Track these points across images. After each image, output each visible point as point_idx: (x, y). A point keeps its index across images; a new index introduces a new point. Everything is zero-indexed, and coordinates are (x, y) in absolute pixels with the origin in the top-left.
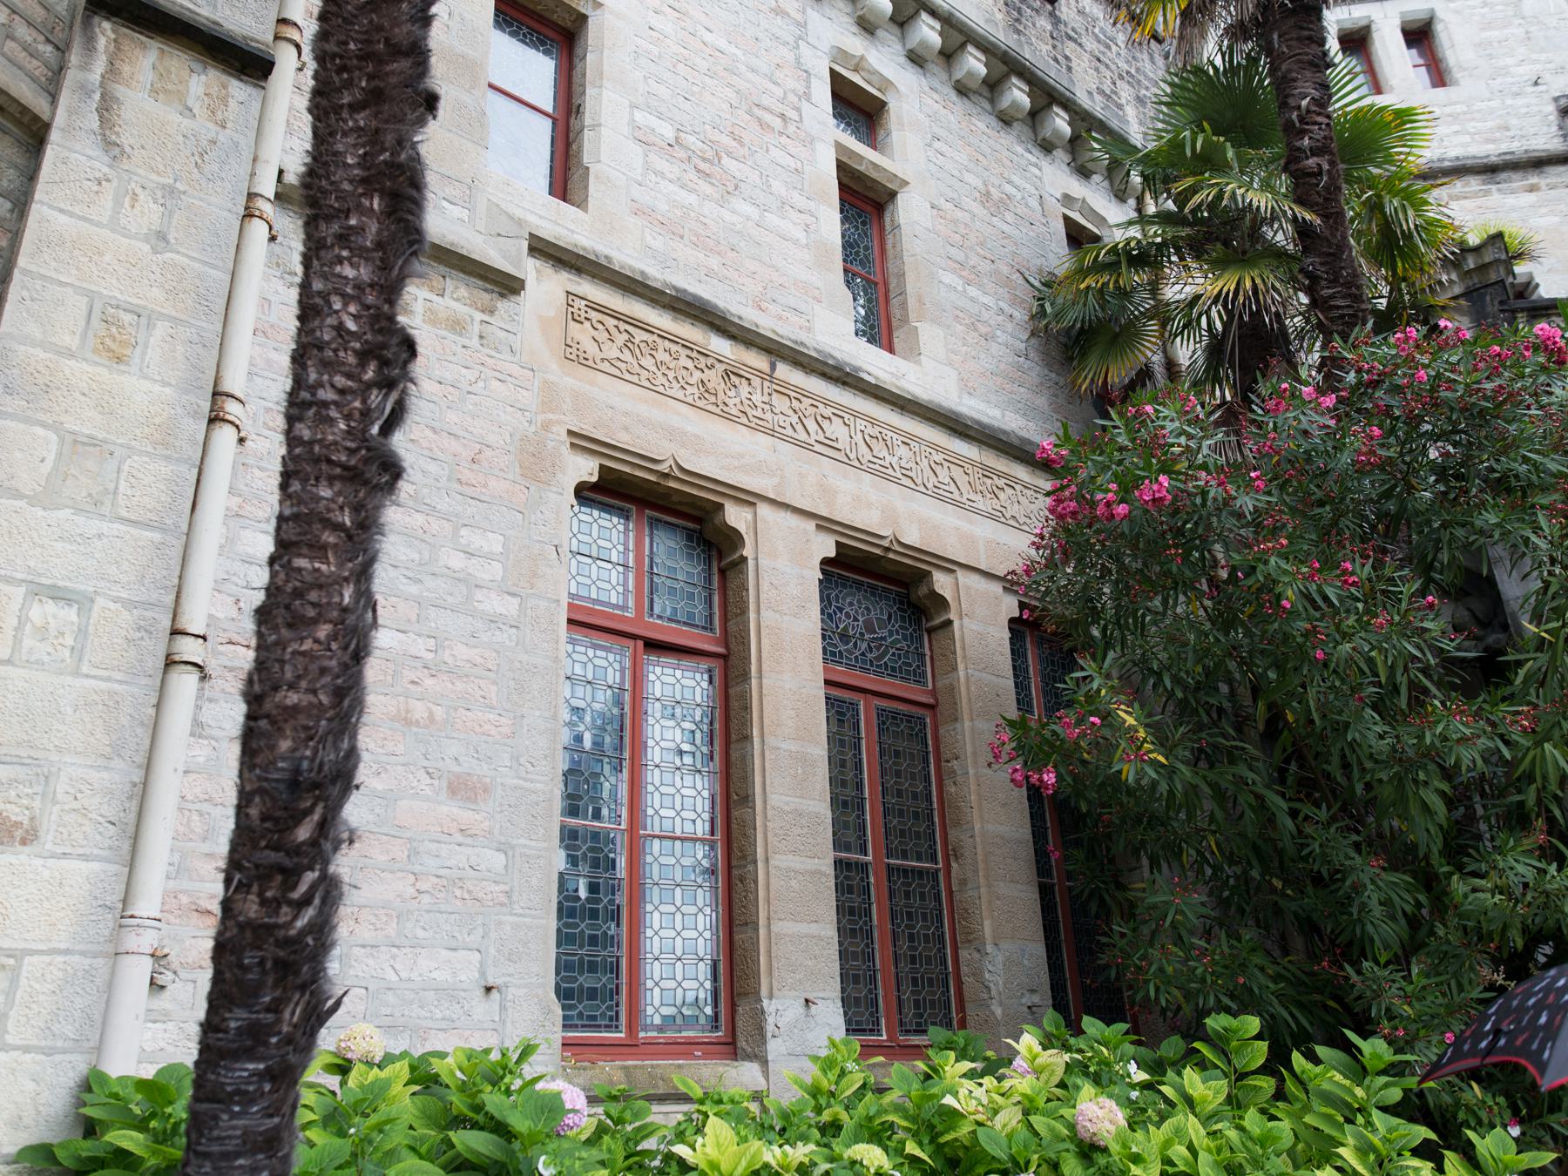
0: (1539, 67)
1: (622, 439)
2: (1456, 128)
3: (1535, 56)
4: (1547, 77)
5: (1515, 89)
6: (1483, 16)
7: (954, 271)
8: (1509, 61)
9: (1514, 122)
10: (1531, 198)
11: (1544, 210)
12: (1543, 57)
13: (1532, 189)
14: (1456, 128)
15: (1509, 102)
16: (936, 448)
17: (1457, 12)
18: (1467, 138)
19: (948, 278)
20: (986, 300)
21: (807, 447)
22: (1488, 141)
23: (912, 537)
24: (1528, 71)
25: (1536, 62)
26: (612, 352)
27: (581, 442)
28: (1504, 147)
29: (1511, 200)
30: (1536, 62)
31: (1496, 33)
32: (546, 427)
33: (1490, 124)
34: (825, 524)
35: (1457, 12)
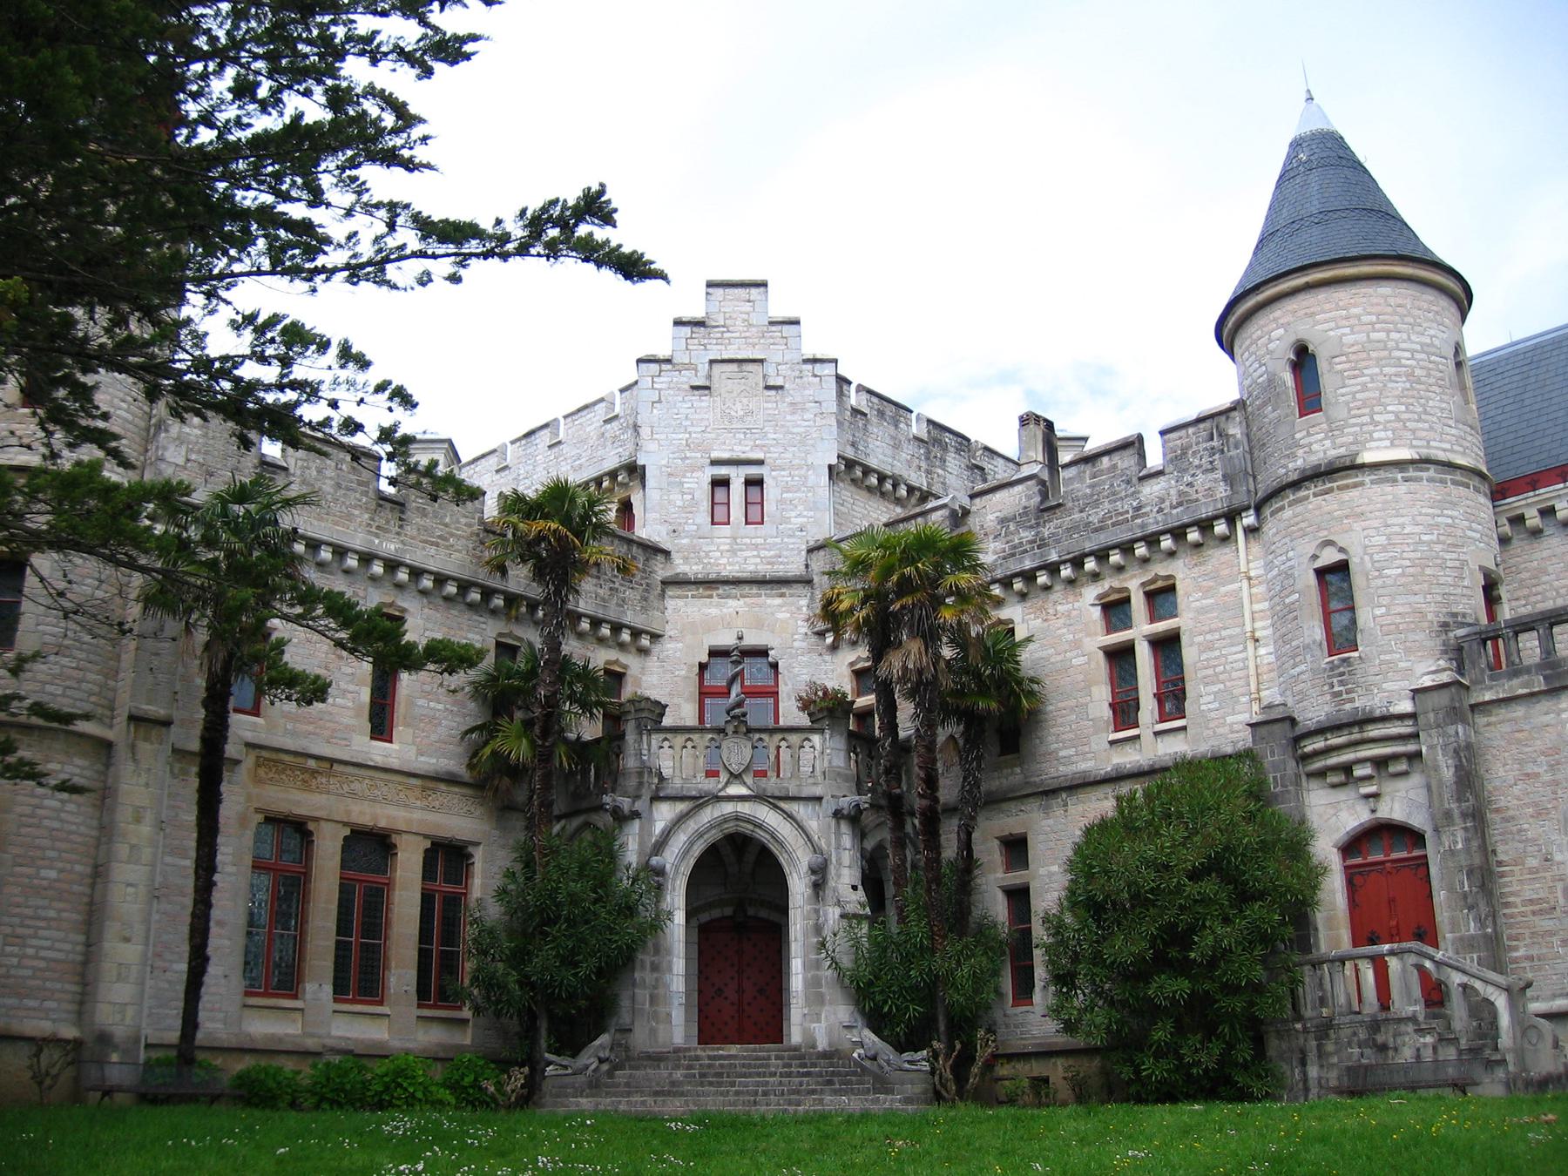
1: (273, 807)
7: (424, 697)
8: (793, 514)
10: (778, 601)
13: (782, 595)
16: (400, 783)
17: (774, 478)
18: (758, 560)
19: (421, 702)
20: (440, 707)
21: (342, 795)
22: (769, 563)
23: (382, 824)
26: (271, 775)
27: (258, 810)
29: (769, 601)
31: (789, 495)
32: (247, 808)
33: (772, 553)
34: (345, 824)
35: (774, 478)
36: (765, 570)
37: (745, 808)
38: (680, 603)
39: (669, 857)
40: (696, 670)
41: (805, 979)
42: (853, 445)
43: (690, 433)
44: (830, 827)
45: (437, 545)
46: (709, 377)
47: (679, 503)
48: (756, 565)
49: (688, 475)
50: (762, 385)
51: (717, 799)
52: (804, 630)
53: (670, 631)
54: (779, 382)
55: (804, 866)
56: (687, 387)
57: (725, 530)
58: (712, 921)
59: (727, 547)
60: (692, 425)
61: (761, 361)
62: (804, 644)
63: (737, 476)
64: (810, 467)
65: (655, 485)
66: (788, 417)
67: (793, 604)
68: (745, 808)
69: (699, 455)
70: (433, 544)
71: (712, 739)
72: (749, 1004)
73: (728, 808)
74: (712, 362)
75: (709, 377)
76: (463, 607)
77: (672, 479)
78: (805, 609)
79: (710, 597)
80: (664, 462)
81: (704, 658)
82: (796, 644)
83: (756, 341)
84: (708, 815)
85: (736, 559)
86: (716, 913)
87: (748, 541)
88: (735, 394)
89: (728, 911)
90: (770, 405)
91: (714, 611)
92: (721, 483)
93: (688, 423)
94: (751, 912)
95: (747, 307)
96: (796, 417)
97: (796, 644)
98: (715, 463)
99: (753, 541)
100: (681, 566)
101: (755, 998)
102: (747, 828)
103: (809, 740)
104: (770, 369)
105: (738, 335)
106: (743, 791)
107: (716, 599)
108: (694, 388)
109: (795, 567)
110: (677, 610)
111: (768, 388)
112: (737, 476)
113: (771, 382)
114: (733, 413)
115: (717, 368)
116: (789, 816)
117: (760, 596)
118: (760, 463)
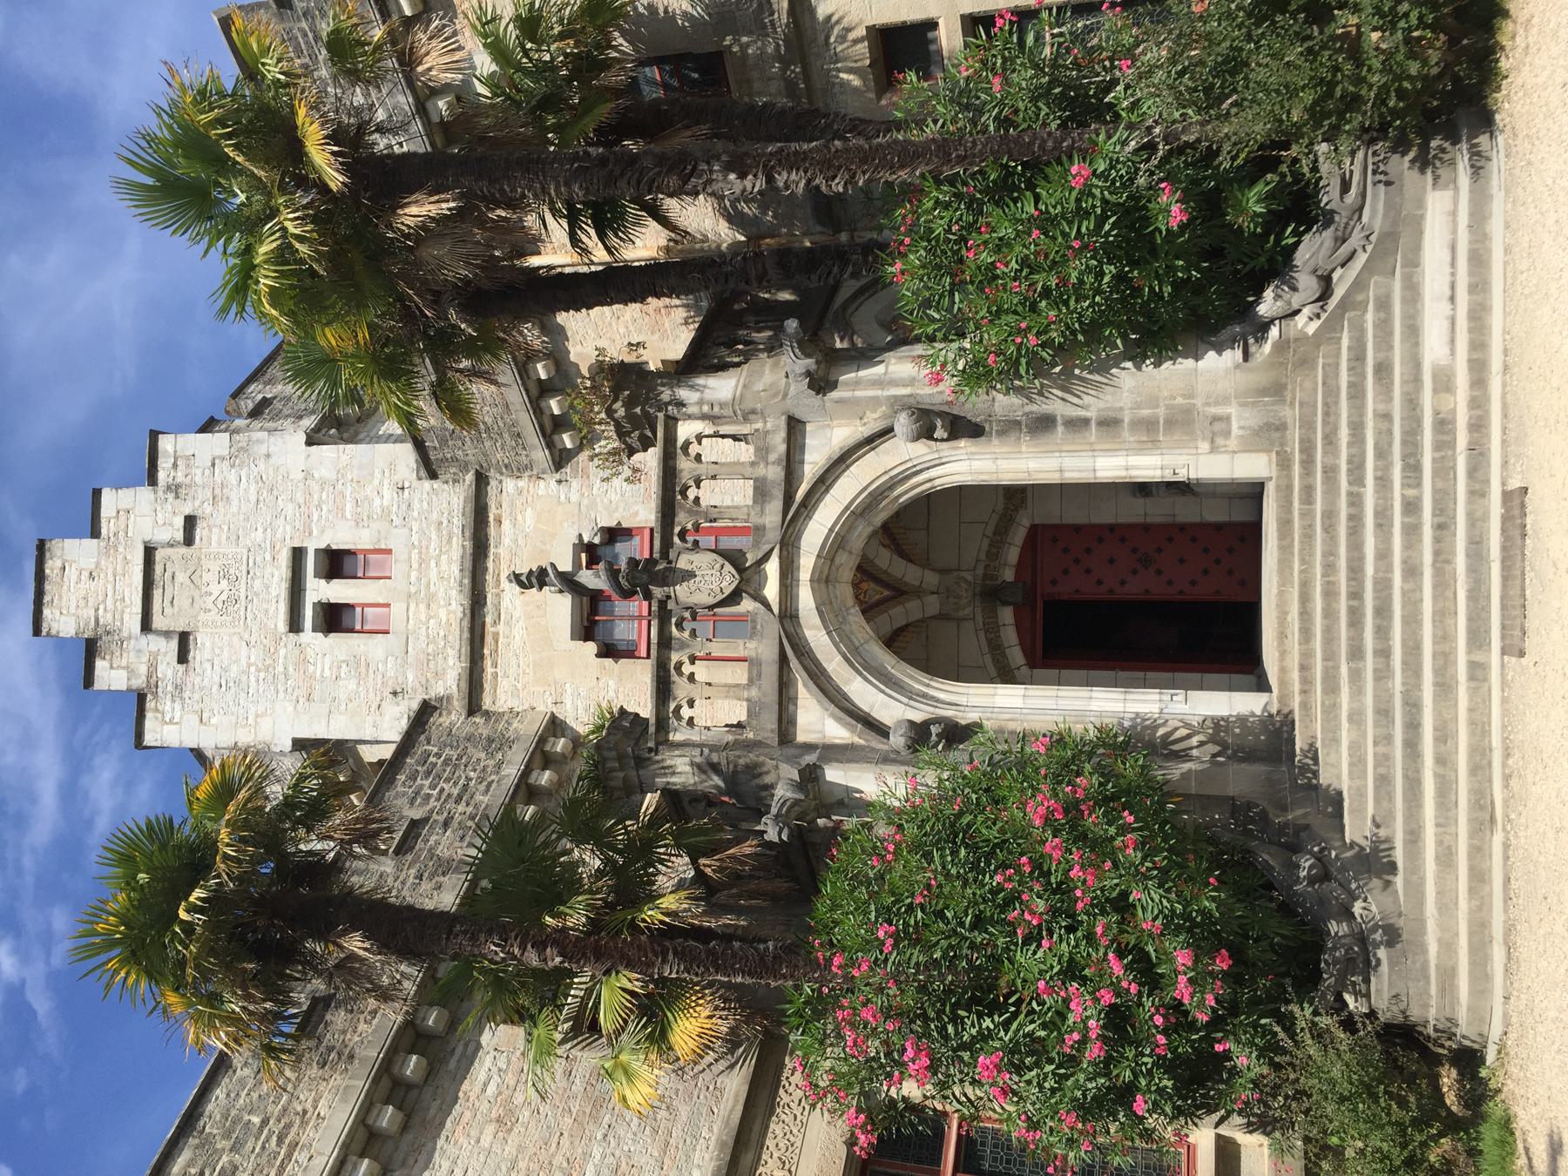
0: (386, 482)
2: (433, 564)
3: (376, 482)
4: (397, 478)
5: (404, 507)
6: (329, 511)
8: (377, 501)
9: (435, 516)
10: (506, 524)
11: (519, 518)
12: (378, 475)
14: (433, 564)
15: (415, 514)
18: (444, 557)
24: (388, 493)
25: (381, 483)
28: (457, 531)
29: (506, 541)
30: (381, 483)
31: (349, 506)
36: (457, 548)
37: (807, 563)
38: (504, 685)
39: (890, 710)
40: (608, 662)
41: (1140, 450)
42: (300, 417)
43: (249, 666)
44: (839, 401)
45: (294, 1146)
46: (167, 634)
47: (352, 686)
48: (450, 562)
49: (311, 668)
50: (184, 550)
51: (788, 615)
52: (553, 484)
53: (545, 707)
54: (179, 522)
55: (921, 451)
56: (181, 668)
57: (397, 610)
58: (1022, 644)
59: (422, 607)
60: (237, 661)
61: (149, 552)
62: (575, 484)
63: (319, 590)
64: (308, 475)
65: (324, 722)
66: (234, 509)
67: (512, 504)
68: (807, 563)
69: (282, 652)
70: (289, 1156)
71: (679, 626)
72: (1170, 583)
73: (806, 599)
74: (146, 626)
75: (167, 634)
76: (428, 1093)
77: (316, 696)
78: (521, 483)
79: (496, 637)
80: (290, 708)
81: (591, 647)
82: (574, 497)
83: (120, 558)
84: (816, 636)
85: (441, 594)
86: (1010, 636)
87: (414, 575)
88: (196, 594)
89: (1007, 615)
90: (214, 538)
91: (518, 633)
92: (334, 618)
93: (234, 668)
94: (1009, 575)
95: (71, 573)
96: (233, 496)
97: (574, 497)
98: (295, 626)
99: (415, 566)
100: (449, 680)
101: (1159, 572)
102: (847, 565)
103: (687, 444)
104: (161, 536)
105: (110, 587)
106: (772, 568)
107: (501, 628)
108: (183, 657)
109: (451, 498)
110: (515, 693)
111: (189, 540)
112: (319, 590)
113: (180, 536)
114: (224, 597)
115: (158, 622)
116: (825, 481)
117: (497, 556)
118: (298, 554)
